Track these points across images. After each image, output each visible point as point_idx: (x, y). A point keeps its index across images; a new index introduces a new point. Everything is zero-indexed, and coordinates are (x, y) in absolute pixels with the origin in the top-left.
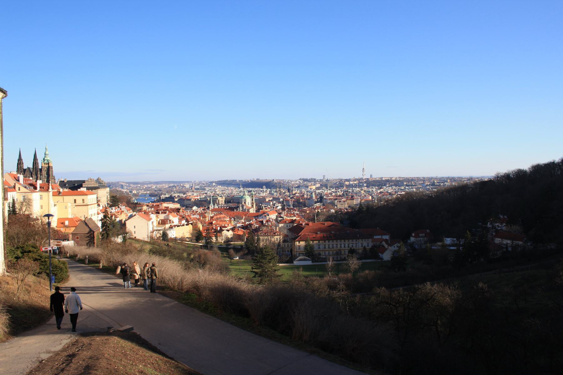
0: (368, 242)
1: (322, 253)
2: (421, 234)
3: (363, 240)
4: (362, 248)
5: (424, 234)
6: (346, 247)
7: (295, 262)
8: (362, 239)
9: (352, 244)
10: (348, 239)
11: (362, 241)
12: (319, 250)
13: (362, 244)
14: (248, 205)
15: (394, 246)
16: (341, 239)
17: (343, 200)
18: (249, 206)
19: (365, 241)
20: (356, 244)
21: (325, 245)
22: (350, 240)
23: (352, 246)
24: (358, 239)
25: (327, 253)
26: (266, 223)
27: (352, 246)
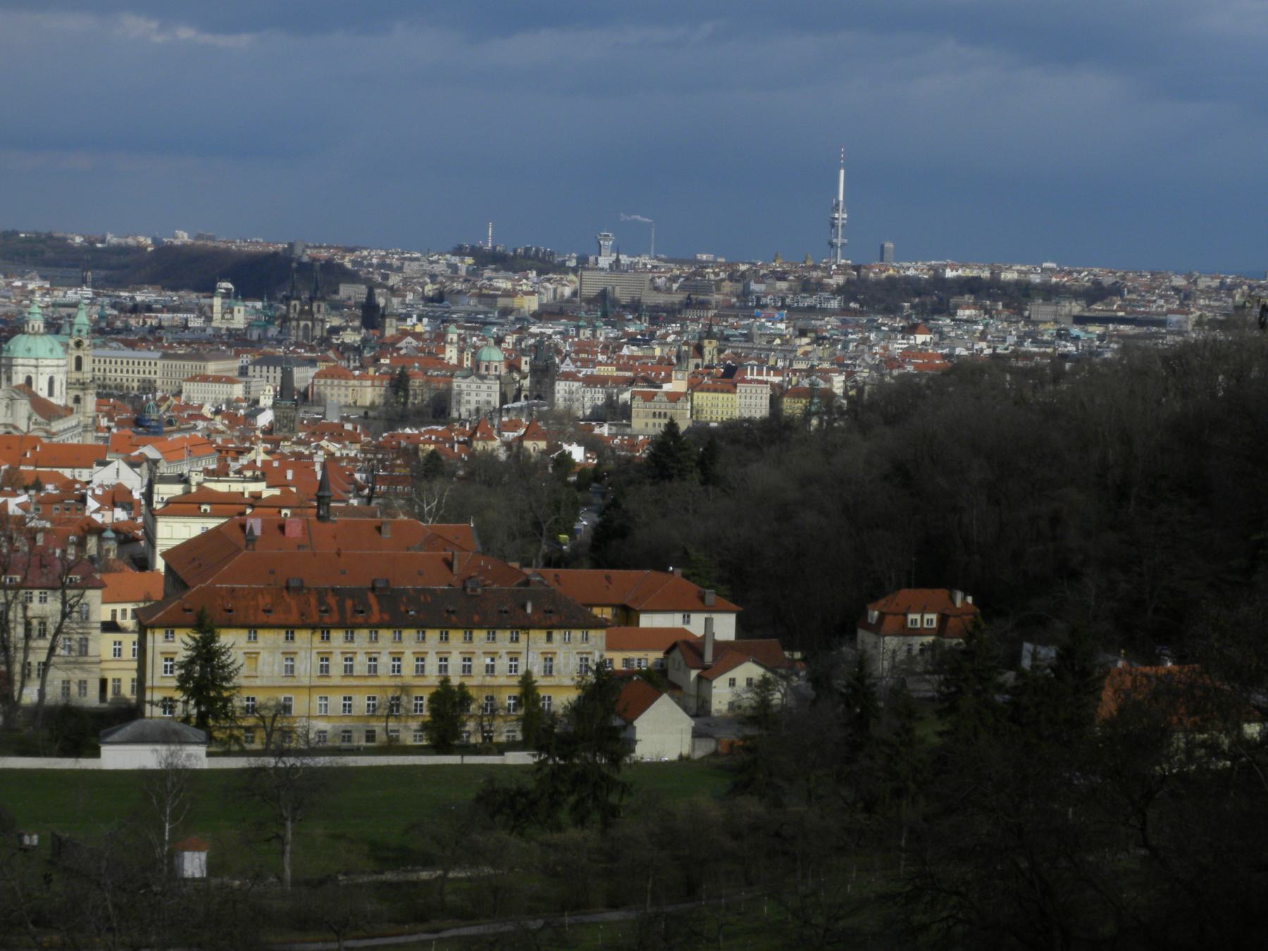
0: (585, 647)
1: (300, 705)
2: (918, 617)
3: (557, 635)
4: (515, 681)
5: (934, 617)
6: (381, 671)
7: (106, 750)
8: (549, 628)
9: (484, 653)
10: (468, 627)
11: (549, 638)
12: (289, 682)
13: (549, 659)
14: (51, 393)
15: (730, 674)
16: (445, 626)
17: (667, 387)
18: (53, 400)
19: (567, 641)
20: (514, 657)
21: (325, 658)
22: (480, 635)
23: (490, 669)
24: (527, 628)
25: (336, 700)
26: (97, 511)
27: (490, 669)
